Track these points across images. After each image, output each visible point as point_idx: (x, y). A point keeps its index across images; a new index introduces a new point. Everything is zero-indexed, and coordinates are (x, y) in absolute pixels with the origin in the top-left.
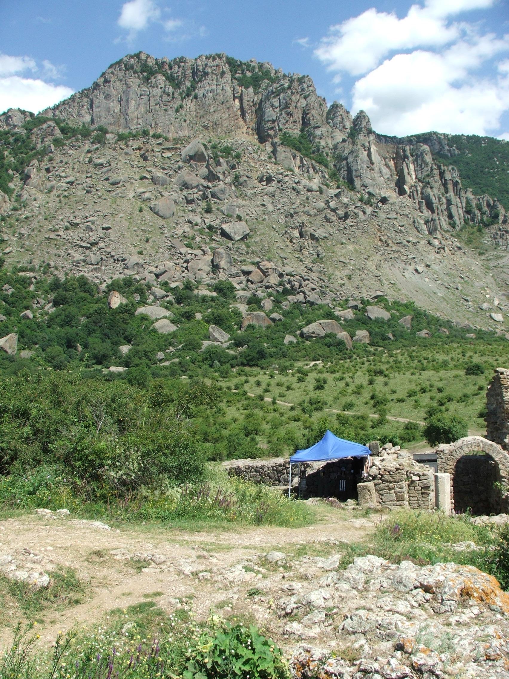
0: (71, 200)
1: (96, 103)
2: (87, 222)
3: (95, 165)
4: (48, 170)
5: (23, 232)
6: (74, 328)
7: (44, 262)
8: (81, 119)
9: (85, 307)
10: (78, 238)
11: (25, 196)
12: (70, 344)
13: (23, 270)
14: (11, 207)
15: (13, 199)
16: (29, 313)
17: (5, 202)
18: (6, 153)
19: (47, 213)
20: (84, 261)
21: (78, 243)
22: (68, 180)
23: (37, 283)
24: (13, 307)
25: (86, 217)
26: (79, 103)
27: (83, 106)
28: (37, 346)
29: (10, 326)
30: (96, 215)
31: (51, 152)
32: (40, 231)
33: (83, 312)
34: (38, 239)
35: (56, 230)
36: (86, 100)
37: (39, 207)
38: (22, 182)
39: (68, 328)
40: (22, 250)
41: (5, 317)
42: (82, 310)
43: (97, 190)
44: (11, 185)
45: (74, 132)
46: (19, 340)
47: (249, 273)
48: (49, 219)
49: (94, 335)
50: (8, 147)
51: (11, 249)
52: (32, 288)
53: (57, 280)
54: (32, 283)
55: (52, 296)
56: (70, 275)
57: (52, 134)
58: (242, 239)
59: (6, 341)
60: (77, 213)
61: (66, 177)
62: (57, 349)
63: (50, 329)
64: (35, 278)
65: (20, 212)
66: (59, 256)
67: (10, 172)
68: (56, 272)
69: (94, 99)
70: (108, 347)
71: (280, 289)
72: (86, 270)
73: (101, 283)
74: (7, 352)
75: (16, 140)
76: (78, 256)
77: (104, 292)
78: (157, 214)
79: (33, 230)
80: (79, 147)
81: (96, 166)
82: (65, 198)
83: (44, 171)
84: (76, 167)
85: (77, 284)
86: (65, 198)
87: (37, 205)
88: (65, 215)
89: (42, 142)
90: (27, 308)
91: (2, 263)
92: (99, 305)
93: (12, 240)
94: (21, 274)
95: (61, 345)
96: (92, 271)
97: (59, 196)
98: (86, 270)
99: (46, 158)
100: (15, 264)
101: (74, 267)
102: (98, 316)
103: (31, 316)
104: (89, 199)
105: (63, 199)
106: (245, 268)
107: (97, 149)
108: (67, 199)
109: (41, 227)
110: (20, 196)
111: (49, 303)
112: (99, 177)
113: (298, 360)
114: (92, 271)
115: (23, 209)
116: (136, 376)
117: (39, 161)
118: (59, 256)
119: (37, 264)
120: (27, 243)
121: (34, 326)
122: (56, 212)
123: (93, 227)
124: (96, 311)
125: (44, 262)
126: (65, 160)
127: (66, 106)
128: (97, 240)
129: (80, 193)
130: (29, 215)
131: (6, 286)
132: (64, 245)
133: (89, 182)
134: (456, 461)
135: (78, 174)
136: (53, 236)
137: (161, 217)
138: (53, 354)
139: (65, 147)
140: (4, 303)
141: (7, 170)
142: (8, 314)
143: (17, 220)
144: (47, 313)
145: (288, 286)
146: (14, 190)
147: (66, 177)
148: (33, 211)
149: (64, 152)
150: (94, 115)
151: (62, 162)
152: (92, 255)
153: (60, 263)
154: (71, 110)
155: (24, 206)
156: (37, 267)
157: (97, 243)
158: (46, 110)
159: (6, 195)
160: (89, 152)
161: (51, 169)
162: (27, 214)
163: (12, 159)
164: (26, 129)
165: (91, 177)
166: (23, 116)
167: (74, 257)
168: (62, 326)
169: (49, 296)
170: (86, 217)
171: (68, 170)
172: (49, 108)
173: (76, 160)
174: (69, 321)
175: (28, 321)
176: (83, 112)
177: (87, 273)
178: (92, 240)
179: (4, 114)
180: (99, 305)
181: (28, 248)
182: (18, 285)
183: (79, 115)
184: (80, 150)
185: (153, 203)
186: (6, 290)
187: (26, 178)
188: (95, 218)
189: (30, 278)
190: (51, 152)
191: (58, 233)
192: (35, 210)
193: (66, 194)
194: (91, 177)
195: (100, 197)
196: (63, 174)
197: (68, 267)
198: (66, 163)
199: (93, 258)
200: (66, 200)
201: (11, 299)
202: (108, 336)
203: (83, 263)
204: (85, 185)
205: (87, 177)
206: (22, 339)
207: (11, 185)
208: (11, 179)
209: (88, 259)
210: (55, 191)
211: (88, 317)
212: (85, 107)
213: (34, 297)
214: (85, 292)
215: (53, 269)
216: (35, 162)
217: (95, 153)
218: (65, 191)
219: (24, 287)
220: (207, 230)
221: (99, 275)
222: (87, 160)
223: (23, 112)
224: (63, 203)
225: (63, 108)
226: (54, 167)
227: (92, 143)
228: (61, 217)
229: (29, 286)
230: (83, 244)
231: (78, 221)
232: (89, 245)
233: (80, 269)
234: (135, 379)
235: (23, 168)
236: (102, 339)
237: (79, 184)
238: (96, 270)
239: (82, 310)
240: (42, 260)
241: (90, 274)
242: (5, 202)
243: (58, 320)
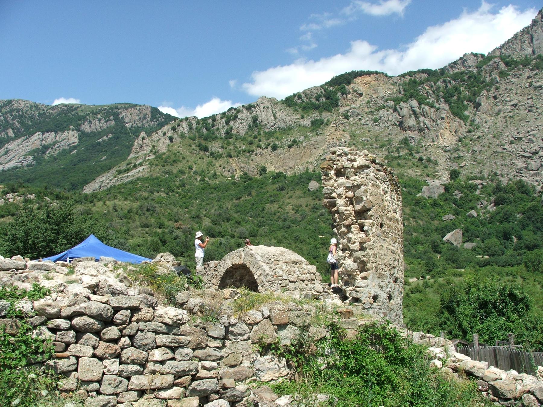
0: (516, 119)
1: (535, 36)
2: (529, 135)
3: (535, 88)
4: (495, 98)
5: (475, 149)
6: (511, 223)
7: (492, 171)
8: (524, 52)
9: (520, 206)
10: (522, 150)
11: (477, 120)
12: (506, 236)
13: (473, 178)
14: (467, 130)
15: (467, 124)
16: (474, 213)
17: (461, 127)
18: (462, 89)
19: (496, 132)
20: (526, 168)
21: (521, 153)
22: (512, 103)
23: (482, 188)
24: (461, 208)
25: (528, 132)
26: (521, 40)
27: (524, 42)
28: (478, 239)
29: (457, 223)
30: (537, 129)
31: (497, 83)
32: (489, 147)
33: (519, 210)
34: (488, 154)
35: (503, 145)
36: (526, 36)
37: (489, 128)
38: (475, 109)
39: (506, 223)
40: (474, 163)
41: (454, 217)
42: (518, 208)
43: (537, 109)
44: (466, 113)
45: (516, 63)
46: (463, 234)
48: (497, 136)
49: (527, 228)
50: (463, 84)
51: (466, 163)
52: (478, 192)
53: (499, 185)
54: (478, 188)
55: (492, 198)
56: (514, 180)
57: (497, 68)
59: (452, 235)
60: (520, 130)
61: (510, 101)
62: (494, 240)
63: (491, 225)
64: (482, 184)
65: (473, 133)
66: (505, 166)
67: (465, 103)
68: (501, 179)
69: (534, 34)
70: (538, 238)
72: (527, 175)
73: (539, 185)
74: (452, 244)
75: (469, 78)
76: (520, 164)
77: (540, 192)
79: (484, 146)
80: (521, 75)
81: (536, 88)
82: (510, 118)
83: (491, 98)
84: (518, 92)
85: (515, 187)
86: (510, 118)
87: (487, 127)
88: (512, 131)
89: (490, 76)
90: (472, 208)
91: (458, 175)
92: (533, 203)
93: (466, 156)
94: (470, 182)
95: (498, 238)
96: (533, 175)
97: (505, 117)
98: (527, 175)
99: (494, 88)
100: (468, 174)
101: (517, 174)
102: (531, 213)
103: (475, 215)
104: (531, 117)
105: (508, 119)
107: (536, 74)
108: (512, 119)
109: (490, 143)
110: (473, 121)
111: (491, 203)
112: (539, 97)
114: (533, 175)
115: (476, 131)
116: (531, 259)
117: (487, 91)
118: (505, 166)
119: (486, 173)
120: (479, 157)
121: (478, 223)
122: (503, 130)
123: (534, 139)
124: (530, 208)
125: (492, 171)
126: (509, 87)
127: (511, 44)
128: (537, 150)
129: (523, 112)
130: (481, 135)
131: (456, 192)
132: (509, 157)
133: (530, 103)
135: (521, 98)
136: (500, 149)
138: (489, 245)
139: (509, 77)
140: (454, 206)
141: (463, 102)
142: (457, 214)
143: (471, 140)
144: (488, 212)
146: (469, 116)
147: (510, 101)
148: (483, 131)
149: (508, 81)
150: (535, 47)
151: (506, 89)
152: (533, 163)
153: (505, 171)
154: (514, 46)
155: (477, 129)
156: (486, 176)
157: (537, 153)
158: (494, 50)
159: (462, 121)
160: (529, 77)
161: (498, 96)
162: (479, 134)
163: (467, 92)
164: (477, 68)
165: (532, 98)
166: (475, 58)
167: (517, 165)
168: (501, 222)
169: (491, 198)
170: (528, 132)
171: (512, 95)
172: (497, 48)
173: (519, 86)
174: (507, 218)
175: (473, 219)
176: (524, 46)
177: (527, 178)
178: (533, 150)
179: (461, 58)
180: (533, 203)
181: (480, 161)
182: (466, 191)
183: (522, 49)
184: (521, 78)
186: (456, 195)
187: (477, 106)
188: (536, 132)
189: (476, 185)
190: (497, 83)
191: (504, 147)
192: (485, 130)
193: (511, 114)
194: (532, 98)
195: (540, 114)
196: (508, 99)
197: (512, 174)
198: (510, 90)
199: (533, 164)
200: (511, 120)
201: (459, 202)
202: (540, 229)
203: (525, 170)
204: (526, 106)
205: (528, 99)
206: (466, 234)
207: (466, 113)
208: (466, 108)
209: (529, 166)
210: (502, 114)
211: (523, 214)
212: (527, 42)
213: (478, 199)
214: (522, 193)
215: (499, 177)
216: (484, 92)
217: (534, 78)
218: (510, 112)
219: (472, 192)
221: (538, 178)
222: (527, 85)
223: (476, 55)
224: (509, 122)
225: (507, 46)
226: (500, 95)
227: (532, 70)
228: (506, 134)
229: (476, 191)
230: (525, 154)
231: (521, 136)
232: (530, 155)
233: (522, 175)
234: (529, 261)
235: (476, 98)
236: (534, 232)
237: (521, 106)
238: (536, 175)
239: (518, 208)
240: (491, 169)
241: (530, 178)
242: (461, 127)
243: (497, 217)
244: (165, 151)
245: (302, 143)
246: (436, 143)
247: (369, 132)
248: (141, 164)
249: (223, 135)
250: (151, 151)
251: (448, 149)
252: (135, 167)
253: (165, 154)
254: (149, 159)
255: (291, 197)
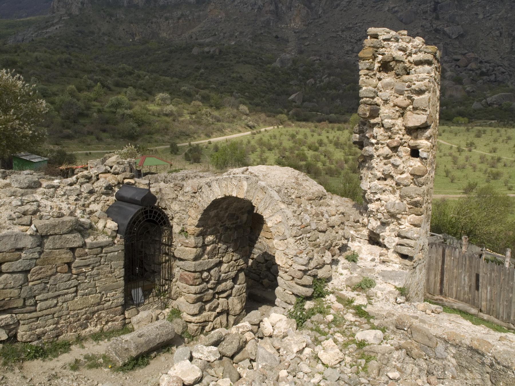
43: (365, 6)
47: (458, 60)
58: (457, 38)
64: (320, 60)
71: (478, 72)
78: (401, 21)
90: (312, 77)
97: (341, 11)
106: (455, 57)
113: (480, 119)
123: (359, 30)
134: (201, 210)
137: (404, 23)
145: (484, 70)
152: (356, 47)
159: (309, 11)
170: (356, 24)
178: (358, 38)
185: (399, 15)
193: (345, 9)
195: (366, 11)
204: (357, 3)
218: (345, 7)
220: (433, 32)
230: (352, 40)
231: (351, 26)
244: (77, 13)
245: (188, 17)
246: (289, 25)
247: (240, 12)
248: (57, 23)
249: (125, 5)
250: (66, 13)
251: (297, 30)
252: (53, 25)
253: (78, 16)
254: (64, 20)
255: (178, 59)
